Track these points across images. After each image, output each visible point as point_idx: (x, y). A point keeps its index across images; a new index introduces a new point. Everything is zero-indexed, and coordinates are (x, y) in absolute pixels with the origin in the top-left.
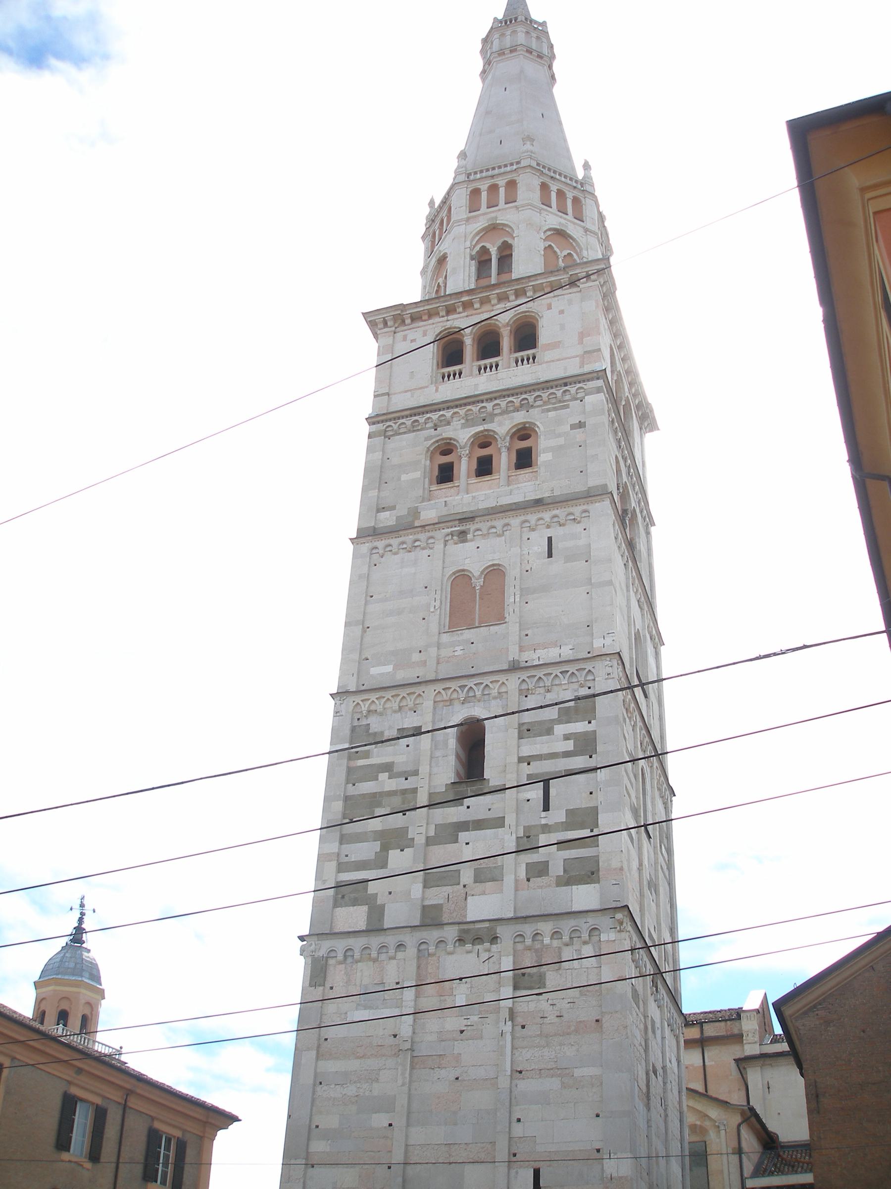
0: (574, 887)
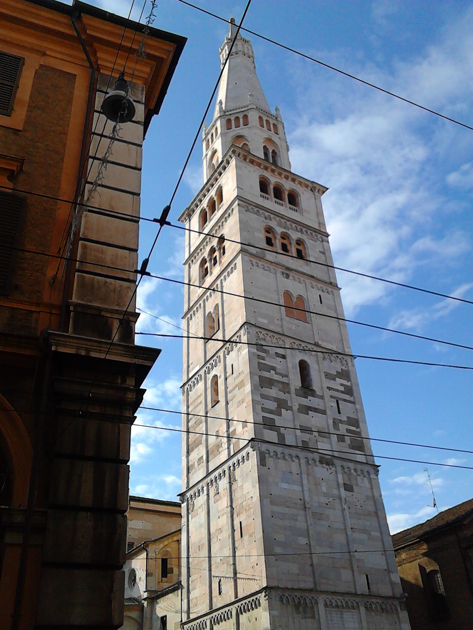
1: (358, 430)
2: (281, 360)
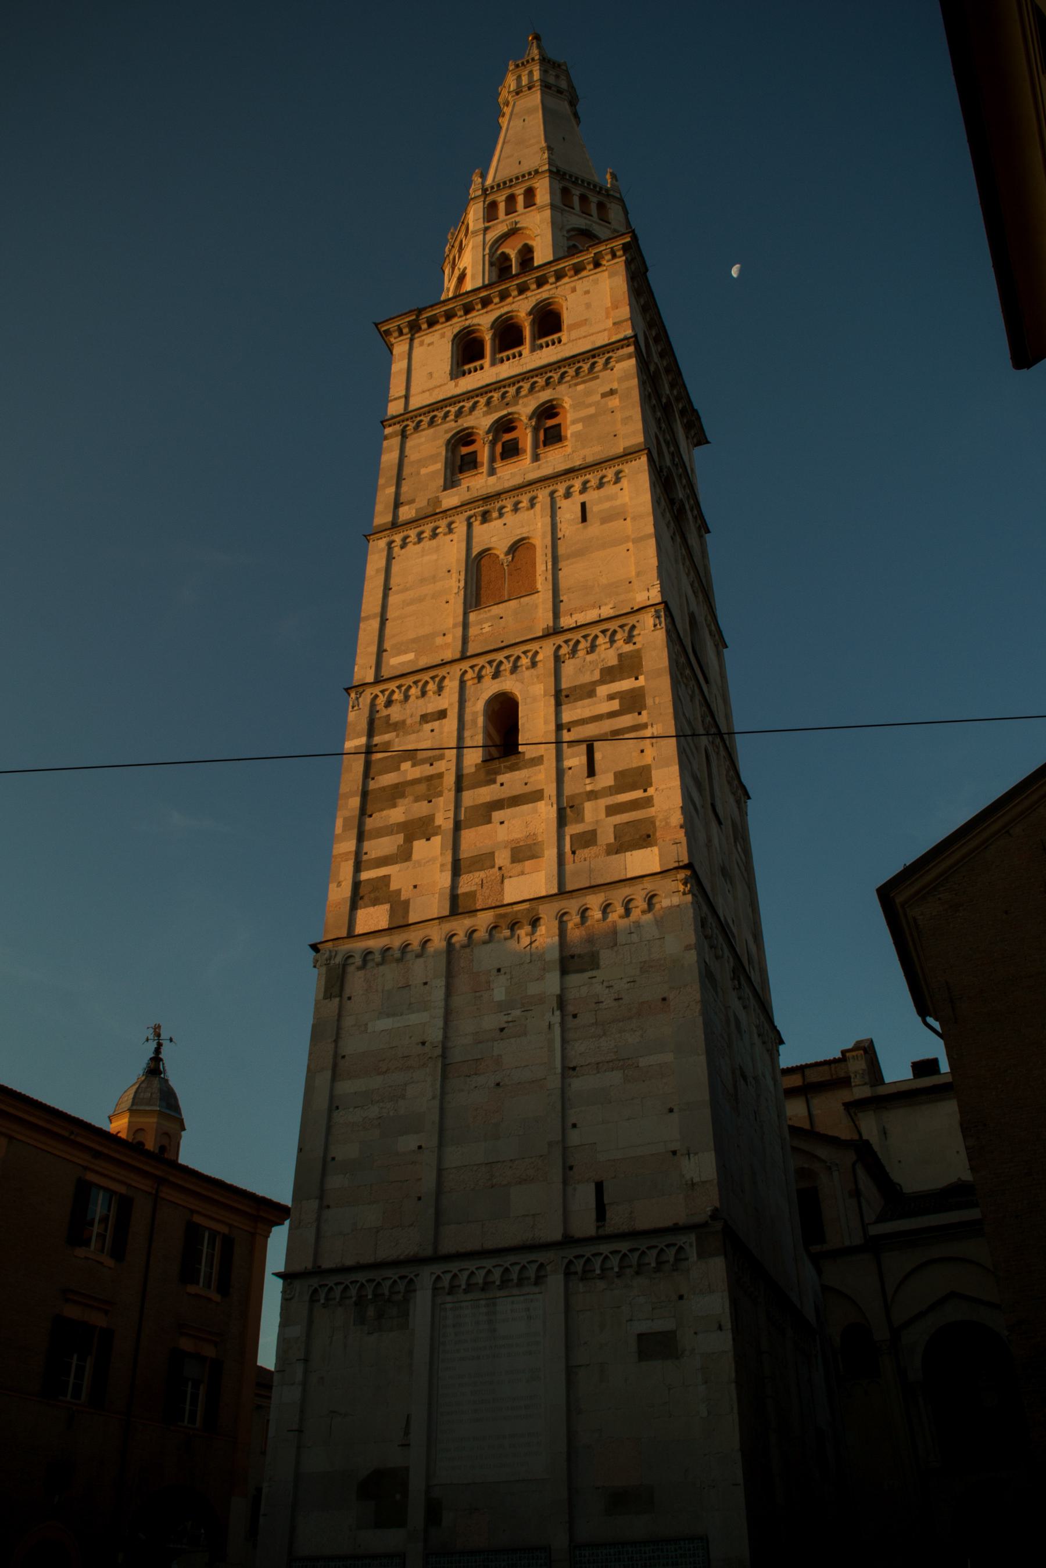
0: (628, 854)
2: (436, 724)
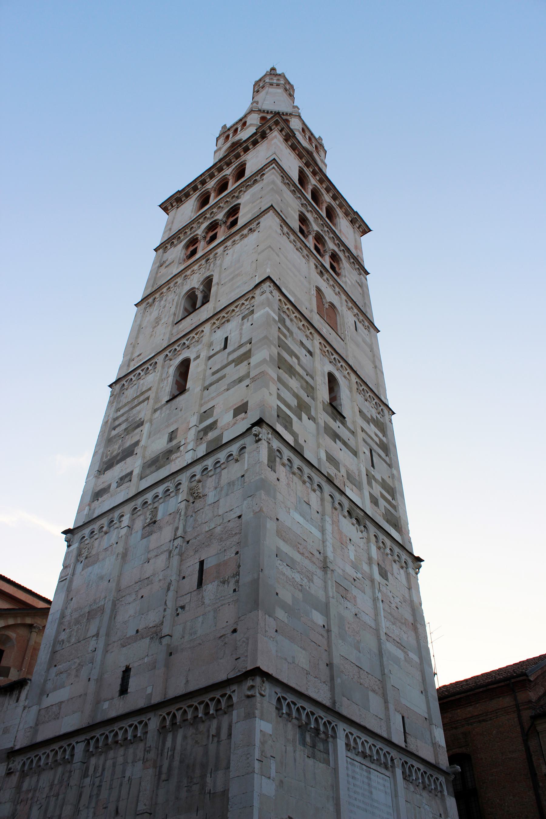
1: (393, 502)
2: (308, 354)
